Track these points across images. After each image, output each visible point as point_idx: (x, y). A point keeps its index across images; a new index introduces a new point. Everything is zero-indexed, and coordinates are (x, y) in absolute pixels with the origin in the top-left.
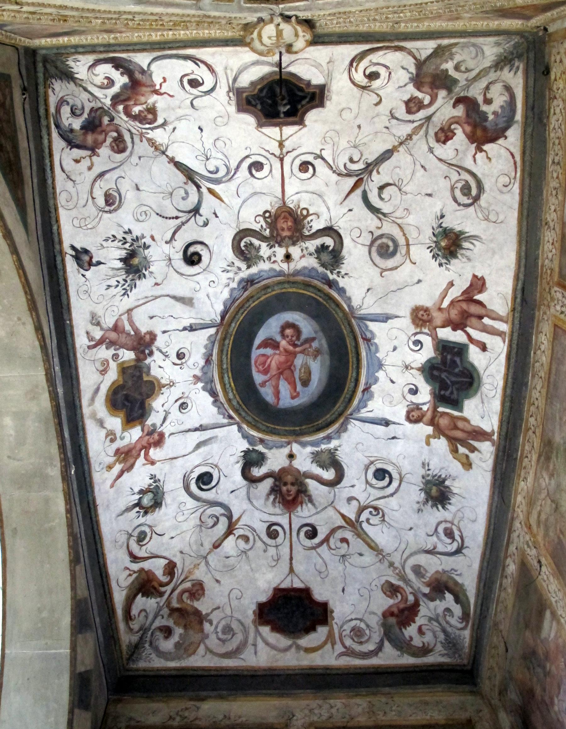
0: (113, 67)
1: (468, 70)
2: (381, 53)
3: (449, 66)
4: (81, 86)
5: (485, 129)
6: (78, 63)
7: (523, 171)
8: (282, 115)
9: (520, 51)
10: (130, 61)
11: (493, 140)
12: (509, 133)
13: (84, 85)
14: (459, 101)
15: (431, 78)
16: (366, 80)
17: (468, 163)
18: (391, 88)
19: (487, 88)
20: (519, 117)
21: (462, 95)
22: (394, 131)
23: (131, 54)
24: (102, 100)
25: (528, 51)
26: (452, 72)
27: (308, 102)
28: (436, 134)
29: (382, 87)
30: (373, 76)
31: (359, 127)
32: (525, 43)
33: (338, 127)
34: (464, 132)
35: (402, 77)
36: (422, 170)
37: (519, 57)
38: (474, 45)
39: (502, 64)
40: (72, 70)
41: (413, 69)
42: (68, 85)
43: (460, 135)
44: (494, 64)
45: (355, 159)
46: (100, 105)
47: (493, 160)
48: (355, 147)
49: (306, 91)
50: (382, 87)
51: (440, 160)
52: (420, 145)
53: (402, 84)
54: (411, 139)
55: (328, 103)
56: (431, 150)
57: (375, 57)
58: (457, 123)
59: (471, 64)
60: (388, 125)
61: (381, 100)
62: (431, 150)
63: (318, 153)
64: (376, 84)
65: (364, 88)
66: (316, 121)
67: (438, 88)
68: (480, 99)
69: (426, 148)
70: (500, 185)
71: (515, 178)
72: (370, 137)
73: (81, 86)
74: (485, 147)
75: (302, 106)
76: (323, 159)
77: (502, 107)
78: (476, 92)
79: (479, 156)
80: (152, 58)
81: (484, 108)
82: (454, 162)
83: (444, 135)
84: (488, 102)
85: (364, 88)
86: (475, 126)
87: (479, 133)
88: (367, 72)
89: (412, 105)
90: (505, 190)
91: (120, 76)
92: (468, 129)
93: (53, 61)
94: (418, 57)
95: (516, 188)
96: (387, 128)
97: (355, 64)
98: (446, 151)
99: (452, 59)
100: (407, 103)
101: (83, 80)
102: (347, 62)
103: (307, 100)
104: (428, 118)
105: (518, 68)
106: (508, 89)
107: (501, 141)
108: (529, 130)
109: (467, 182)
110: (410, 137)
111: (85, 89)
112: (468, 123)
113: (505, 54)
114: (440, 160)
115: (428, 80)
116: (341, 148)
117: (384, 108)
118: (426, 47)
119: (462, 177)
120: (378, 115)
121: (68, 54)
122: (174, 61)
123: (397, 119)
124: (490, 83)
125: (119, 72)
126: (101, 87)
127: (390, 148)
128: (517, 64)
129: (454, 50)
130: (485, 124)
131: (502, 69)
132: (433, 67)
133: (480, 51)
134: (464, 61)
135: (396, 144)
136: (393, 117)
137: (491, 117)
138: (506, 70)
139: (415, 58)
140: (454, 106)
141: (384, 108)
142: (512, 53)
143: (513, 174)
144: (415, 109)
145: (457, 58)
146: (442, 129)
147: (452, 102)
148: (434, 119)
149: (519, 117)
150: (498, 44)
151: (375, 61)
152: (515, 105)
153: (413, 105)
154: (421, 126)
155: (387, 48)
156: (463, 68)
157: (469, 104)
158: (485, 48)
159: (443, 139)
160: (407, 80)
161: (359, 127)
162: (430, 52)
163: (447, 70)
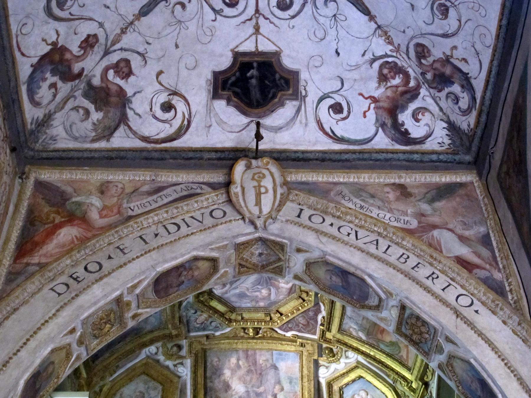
0: (410, 134)
1: (76, 109)
2: (162, 135)
3: (96, 116)
4: (445, 114)
5: (52, 62)
6: (440, 140)
7: (11, 47)
8: (255, 65)
9: (33, 136)
10: (393, 140)
11: (43, 58)
12: (31, 70)
13: (441, 114)
14: (79, 75)
15: (111, 101)
16: (173, 102)
17: (62, 27)
18: (149, 92)
19: (55, 96)
20: (24, 89)
21: (77, 81)
22: (140, 39)
23: (390, 147)
24: (428, 94)
25: (26, 141)
26: (91, 107)
27: (228, 79)
28: (97, 41)
29: (157, 92)
30: (167, 107)
31: (177, 46)
32: (29, 144)
33: (199, 47)
34: (71, 52)
35: (139, 105)
36: (108, 4)
37: (32, 132)
38: (76, 139)
39: (45, 120)
40: (448, 133)
41: (130, 113)
42: (456, 121)
43: (75, 49)
44: (53, 117)
45: (178, 7)
46: (432, 90)
47: (39, 40)
48: (180, 21)
49: (231, 93)
50: (157, 92)
51: (91, 19)
52: (113, 26)
53: (138, 95)
54: (122, 29)
55: (210, 76)
56: (101, 25)
57: (168, 130)
58: (78, 57)
59: (75, 116)
60: (146, 46)
61: (157, 78)
62: (101, 25)
63: (218, 17)
64: (163, 98)
65: (175, 93)
66: (221, 55)
67: (101, 88)
68: (60, 84)
69: (106, 25)
70: (30, 22)
71: (17, 36)
72: (165, 33)
73: (445, 114)
74: (50, 47)
75: (234, 75)
76: (213, 9)
77: (40, 87)
78: (65, 88)
79: (54, 38)
80: (373, 142)
81: (55, 79)
82: (77, 22)
83: (89, 43)
84: (53, 86)
85: (175, 93)
86: (62, 61)
87: (57, 57)
88: (173, 111)
89: (125, 70)
90: (24, 21)
91: (406, 122)
92: (68, 56)
93: (462, 145)
94: (126, 127)
95: (14, 28)
96: (148, 43)
97: (186, 122)
98: (86, 29)
99: (94, 124)
100: (130, 73)
101: (441, 120)
102: (193, 125)
103: (230, 82)
104: (107, 53)
105: (31, 124)
106: (36, 104)
107: (35, 60)
108: (12, 84)
109: (62, 10)
110: (123, 31)
111: (441, 109)
112: (67, 60)
113: (44, 128)
114: (91, 19)
115: (113, 99)
116: (195, 21)
117: (153, 68)
118: (121, 140)
119: (67, 12)
120: (159, 59)
121: (447, 153)
122: (353, 137)
123: (138, 53)
124: (53, 100)
125: (405, 127)
126: (426, 109)
127: (142, 18)
128: (33, 126)
129: (94, 134)
130: (53, 67)
131: (45, 116)
132: (110, 115)
133: (69, 130)
134: (82, 121)
135: (136, 23)
136: (142, 55)
137: (48, 75)
138: (41, 116)
139: (129, 127)
140: (83, 69)
141: (153, 68)
142: (38, 132)
143: (19, 39)
144: (122, 65)
145: (88, 125)
146: (92, 46)
147: (85, 73)
148: (102, 53)
149: (24, 89)
150: (54, 139)
151: (167, 126)
152: (28, 95)
153: (124, 69)
154: (113, 44)
155: (157, 142)
156: (81, 112)
157: (68, 76)
158: (63, 134)
159: (91, 39)
160: (133, 100)
161: (177, 46)
162: (117, 134)
163: (97, 110)
